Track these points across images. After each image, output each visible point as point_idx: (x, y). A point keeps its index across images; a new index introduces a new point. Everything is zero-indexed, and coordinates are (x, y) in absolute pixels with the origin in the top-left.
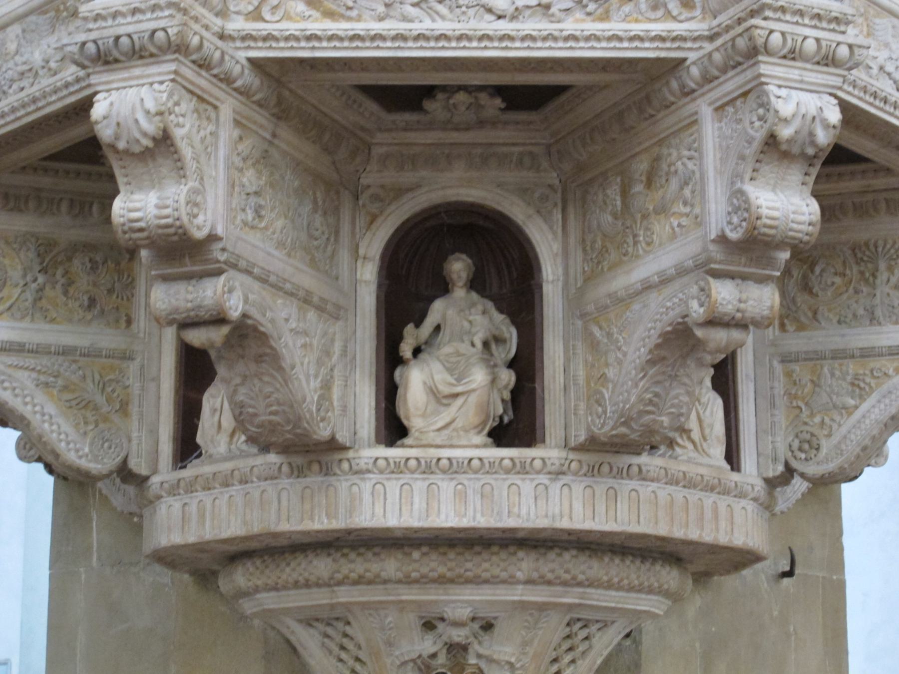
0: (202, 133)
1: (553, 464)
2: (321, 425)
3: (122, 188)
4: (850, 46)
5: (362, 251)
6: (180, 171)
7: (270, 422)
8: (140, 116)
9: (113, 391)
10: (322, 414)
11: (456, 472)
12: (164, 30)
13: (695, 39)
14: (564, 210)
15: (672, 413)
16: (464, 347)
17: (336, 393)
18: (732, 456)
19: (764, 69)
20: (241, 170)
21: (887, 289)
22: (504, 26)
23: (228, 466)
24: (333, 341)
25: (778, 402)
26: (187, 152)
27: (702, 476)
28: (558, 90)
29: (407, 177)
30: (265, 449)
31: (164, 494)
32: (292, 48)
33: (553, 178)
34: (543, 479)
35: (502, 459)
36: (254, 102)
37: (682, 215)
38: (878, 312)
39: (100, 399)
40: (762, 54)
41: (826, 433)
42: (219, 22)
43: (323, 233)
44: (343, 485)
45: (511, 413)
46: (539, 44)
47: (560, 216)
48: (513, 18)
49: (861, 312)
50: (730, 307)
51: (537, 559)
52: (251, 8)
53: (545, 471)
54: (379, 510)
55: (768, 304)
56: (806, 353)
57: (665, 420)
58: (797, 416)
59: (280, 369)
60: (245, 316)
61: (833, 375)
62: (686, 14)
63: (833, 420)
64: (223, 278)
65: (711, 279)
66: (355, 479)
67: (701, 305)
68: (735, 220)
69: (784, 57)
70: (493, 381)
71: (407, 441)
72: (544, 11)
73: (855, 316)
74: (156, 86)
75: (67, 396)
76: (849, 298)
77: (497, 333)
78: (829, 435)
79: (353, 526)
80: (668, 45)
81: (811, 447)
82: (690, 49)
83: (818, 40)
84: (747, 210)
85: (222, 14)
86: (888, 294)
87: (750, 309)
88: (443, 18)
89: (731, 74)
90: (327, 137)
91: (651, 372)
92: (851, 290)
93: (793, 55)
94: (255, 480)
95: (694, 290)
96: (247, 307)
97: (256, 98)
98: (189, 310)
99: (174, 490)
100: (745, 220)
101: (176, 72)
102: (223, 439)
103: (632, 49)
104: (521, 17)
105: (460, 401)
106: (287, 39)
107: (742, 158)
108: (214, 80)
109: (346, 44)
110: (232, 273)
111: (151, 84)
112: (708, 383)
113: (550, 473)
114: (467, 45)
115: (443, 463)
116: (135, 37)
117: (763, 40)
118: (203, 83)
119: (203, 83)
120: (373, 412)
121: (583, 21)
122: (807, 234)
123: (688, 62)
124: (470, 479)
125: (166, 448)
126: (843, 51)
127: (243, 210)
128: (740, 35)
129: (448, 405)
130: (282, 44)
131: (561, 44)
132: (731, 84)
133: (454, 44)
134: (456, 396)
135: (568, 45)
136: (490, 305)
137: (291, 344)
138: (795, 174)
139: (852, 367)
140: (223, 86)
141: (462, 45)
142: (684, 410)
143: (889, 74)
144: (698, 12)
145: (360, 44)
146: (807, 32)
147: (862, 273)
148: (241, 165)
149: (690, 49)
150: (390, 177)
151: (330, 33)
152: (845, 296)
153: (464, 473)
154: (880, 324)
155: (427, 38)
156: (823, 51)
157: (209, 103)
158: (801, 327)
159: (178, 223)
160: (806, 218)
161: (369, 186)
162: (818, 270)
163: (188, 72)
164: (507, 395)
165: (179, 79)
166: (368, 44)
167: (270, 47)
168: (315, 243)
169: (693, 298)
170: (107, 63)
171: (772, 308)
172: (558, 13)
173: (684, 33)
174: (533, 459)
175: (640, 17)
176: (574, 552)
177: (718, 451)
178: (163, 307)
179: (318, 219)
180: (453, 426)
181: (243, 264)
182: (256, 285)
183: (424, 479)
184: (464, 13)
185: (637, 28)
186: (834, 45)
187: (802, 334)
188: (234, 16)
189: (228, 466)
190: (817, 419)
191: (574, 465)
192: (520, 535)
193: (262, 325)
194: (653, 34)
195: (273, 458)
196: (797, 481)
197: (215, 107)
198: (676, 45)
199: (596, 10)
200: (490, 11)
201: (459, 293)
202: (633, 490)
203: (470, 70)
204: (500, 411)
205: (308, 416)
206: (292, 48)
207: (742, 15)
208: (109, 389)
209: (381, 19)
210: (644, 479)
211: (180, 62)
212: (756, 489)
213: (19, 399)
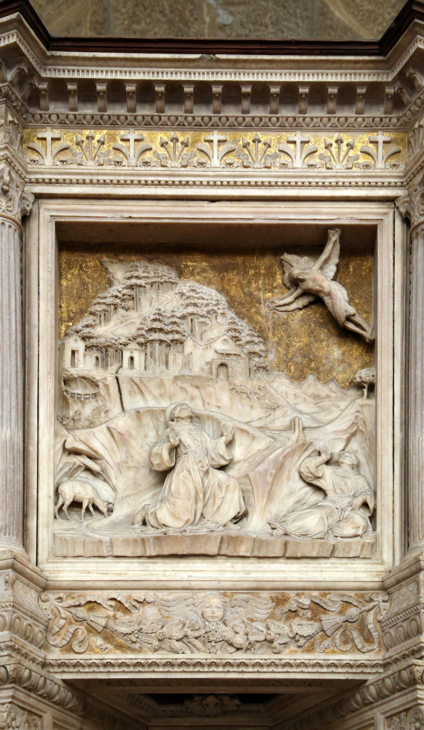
13: (373, 666)
22: (241, 656)
32: (94, 672)
40: (419, 684)
46: (265, 669)
48: (248, 649)
52: (64, 642)
62: (368, 647)
72: (269, 645)
80: (354, 670)
85: (45, 646)
88: (198, 650)
103: (329, 673)
104: (252, 649)
108: (40, 698)
109: (131, 669)
114: (216, 670)
117: (420, 674)
121: (296, 651)
128: (405, 669)
130: (87, 670)
131: (280, 669)
133: (206, 669)
135: (285, 670)
140: (46, 701)
141: (211, 670)
144: (375, 646)
145: (141, 669)
151: (120, 661)
155: (188, 665)
165: (15, 701)
166: (146, 669)
167: (79, 672)
172: (278, 646)
173: (365, 662)
175: (335, 650)
188: (53, 648)
194: (344, 662)
197: (40, 717)
198: (359, 670)
199: (305, 643)
200: (231, 645)
203: (217, 685)
206: (94, 672)
207: (407, 652)
209: (156, 650)
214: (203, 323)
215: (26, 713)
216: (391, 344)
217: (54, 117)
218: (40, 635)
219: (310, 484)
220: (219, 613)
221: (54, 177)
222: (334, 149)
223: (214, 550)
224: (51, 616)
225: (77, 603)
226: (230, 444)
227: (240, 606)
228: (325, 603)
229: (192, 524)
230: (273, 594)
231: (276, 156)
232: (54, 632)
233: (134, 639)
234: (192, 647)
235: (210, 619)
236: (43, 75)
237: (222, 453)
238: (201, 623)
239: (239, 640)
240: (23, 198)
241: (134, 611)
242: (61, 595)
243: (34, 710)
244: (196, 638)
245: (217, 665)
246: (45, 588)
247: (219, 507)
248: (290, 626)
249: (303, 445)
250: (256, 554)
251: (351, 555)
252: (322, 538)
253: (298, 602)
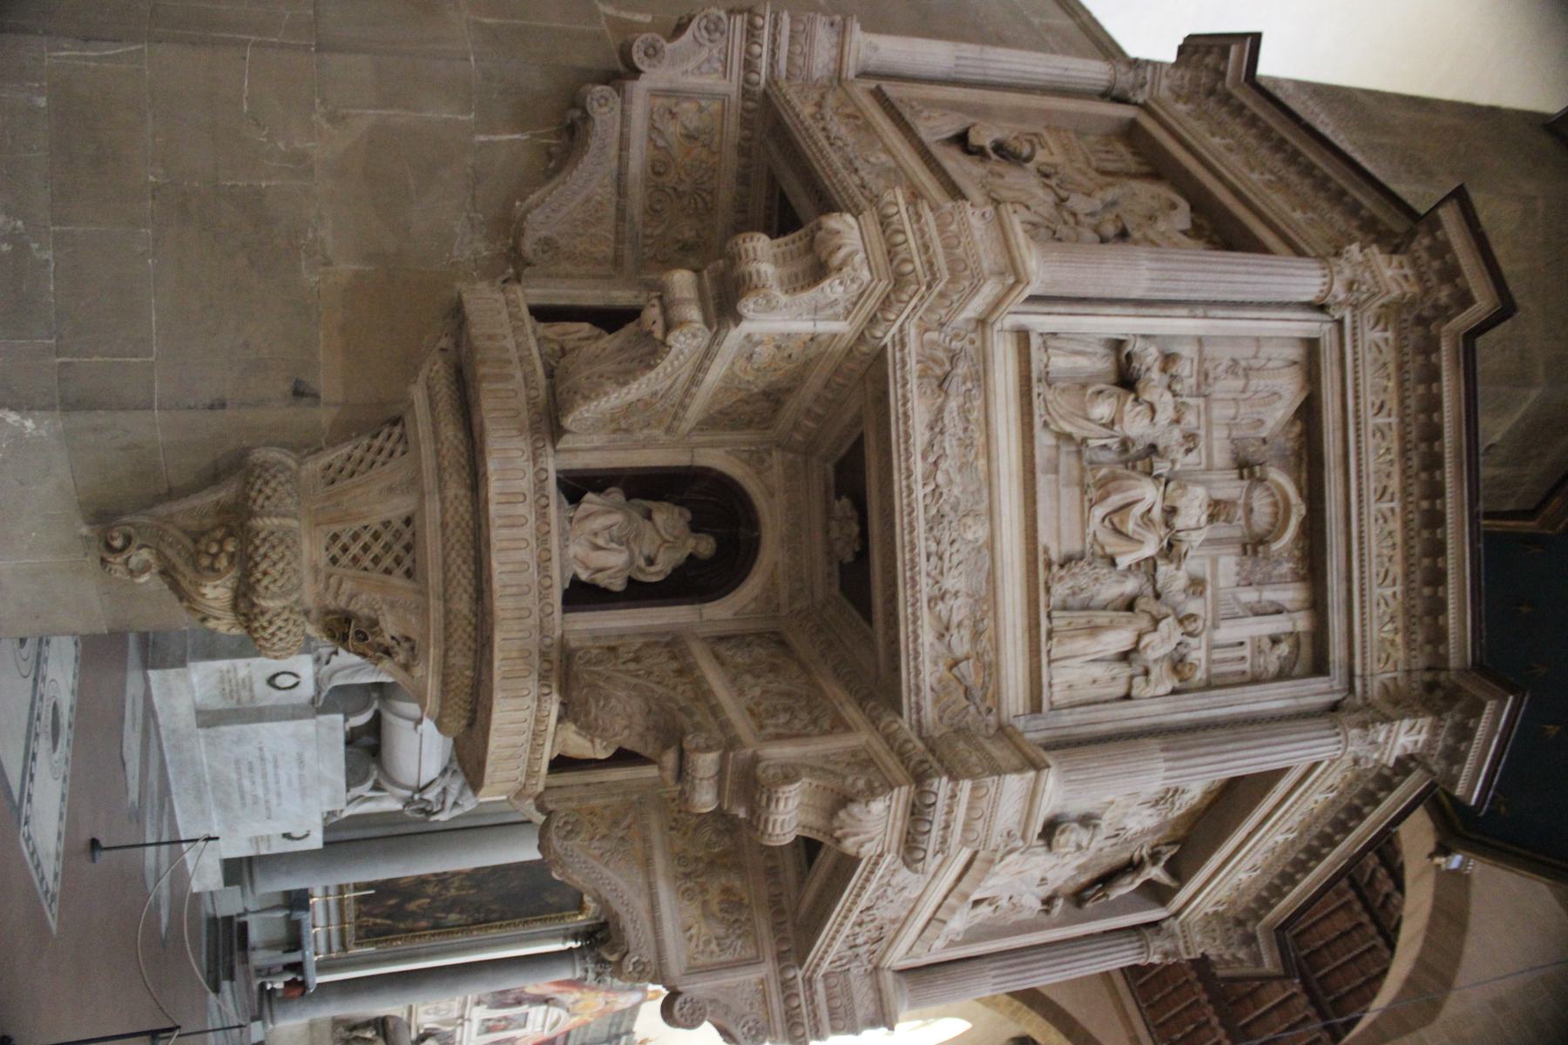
28: (866, 612)
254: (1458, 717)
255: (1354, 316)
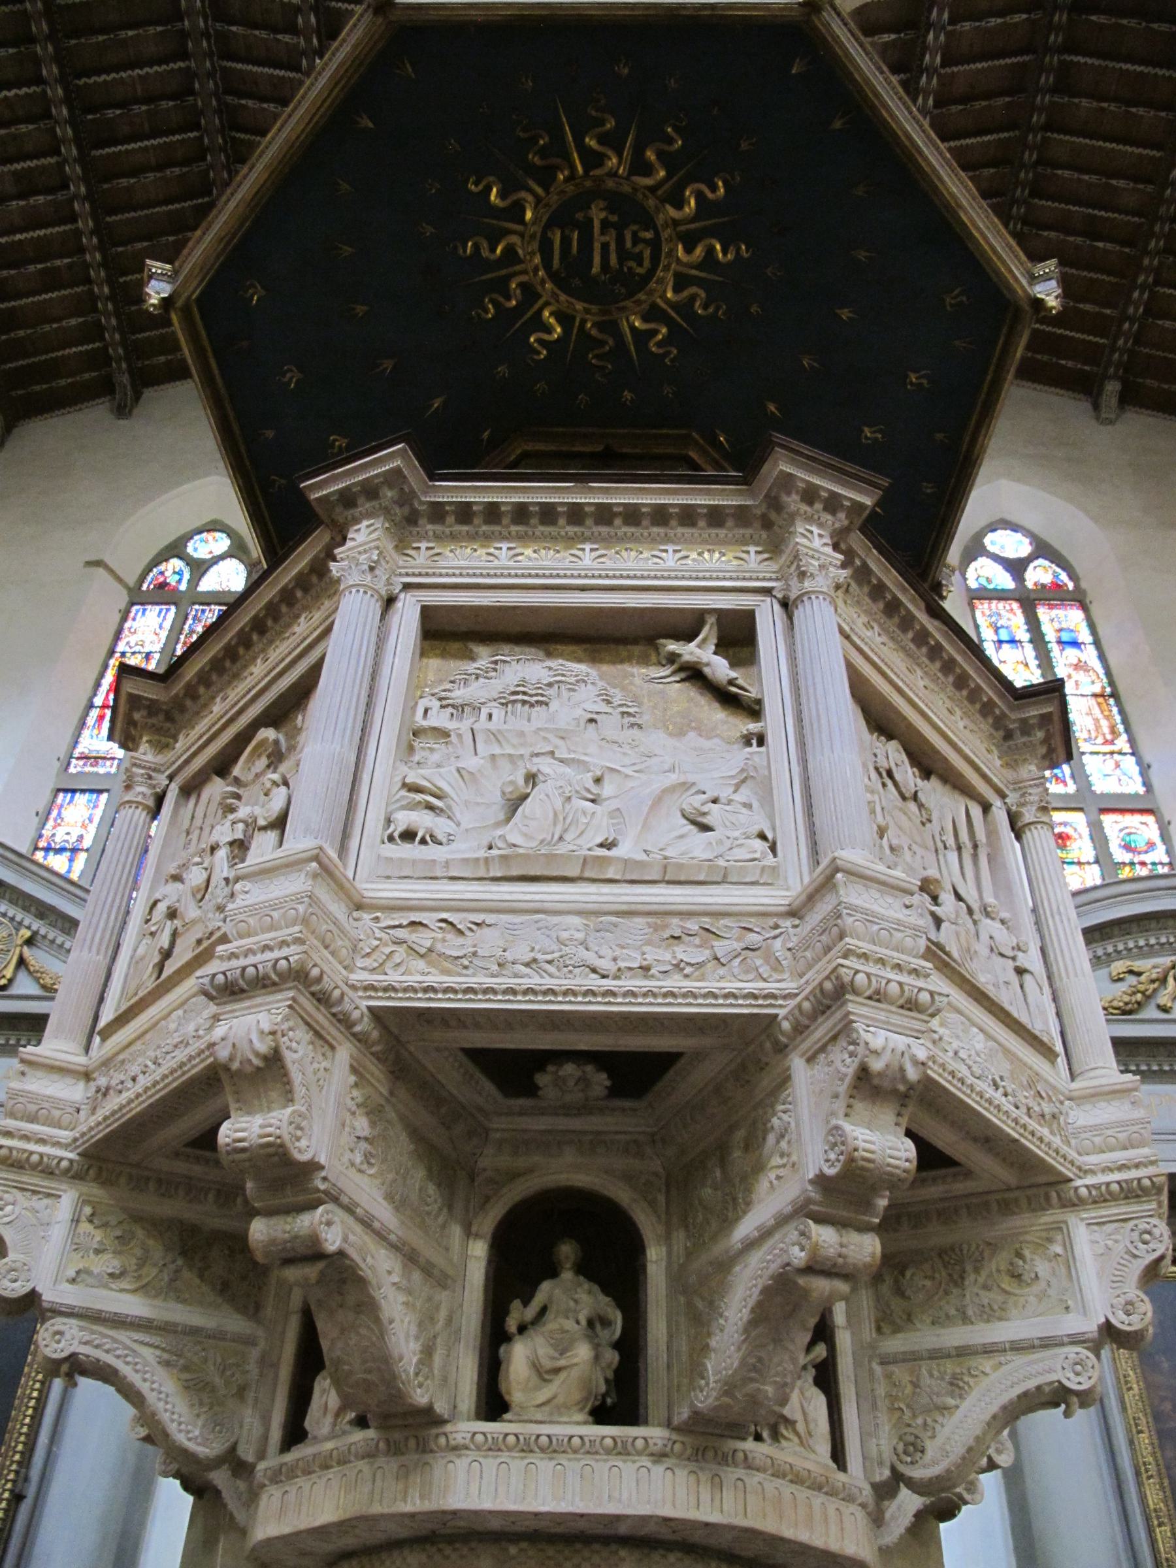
0: (316, 1065)
1: (655, 1444)
2: (419, 1391)
3: (232, 1114)
4: (932, 994)
5: (474, 1229)
6: (288, 1097)
7: (365, 1380)
8: (254, 1037)
9: (233, 1375)
10: (421, 1379)
11: (555, 1451)
12: (286, 958)
14: (668, 1192)
15: (775, 1382)
16: (569, 1324)
17: (437, 1360)
18: (838, 1455)
19: (851, 1007)
20: (354, 1113)
21: (975, 1290)
23: (329, 1445)
24: (437, 1308)
25: (879, 1403)
26: (296, 1077)
27: (809, 1471)
29: (521, 1162)
30: (361, 1422)
31: (267, 1482)
33: (656, 1165)
34: (646, 1461)
35: (603, 1438)
36: (372, 1054)
37: (779, 1167)
38: (970, 1312)
39: (218, 1381)
41: (929, 1434)
42: (344, 972)
43: (436, 1201)
44: (439, 1466)
45: (614, 1395)
47: (663, 1200)
48: (616, 978)
49: (953, 1312)
50: (832, 1250)
51: (641, 1560)
53: (647, 1452)
54: (474, 1489)
55: (870, 1249)
56: (904, 1353)
57: (770, 1390)
58: (900, 1418)
59: (377, 1320)
60: (341, 1253)
61: (931, 1376)
62: (776, 976)
63: (936, 1421)
64: (321, 1209)
65: (810, 1222)
66: (451, 1456)
67: (802, 1249)
68: (832, 1156)
69: (870, 998)
70: (597, 1358)
71: (506, 1416)
73: (947, 1316)
74: (274, 1011)
75: (186, 1376)
76: (940, 1300)
77: (602, 1313)
78: (933, 1437)
79: (446, 1508)
80: (760, 1002)
81: (916, 1450)
82: (781, 1006)
83: (900, 984)
84: (843, 1143)
86: (977, 1294)
87: (851, 1253)
88: (551, 976)
89: (820, 1020)
90: (443, 1110)
91: (753, 1334)
92: (941, 1292)
93: (878, 997)
94: (352, 1459)
95: (794, 1235)
96: (346, 1246)
97: (376, 1049)
98: (285, 1242)
99: (278, 1476)
100: (842, 1154)
101: (294, 999)
102: (329, 1419)
105: (563, 1375)
106: (405, 990)
107: (836, 1096)
109: (460, 996)
110: (330, 1206)
111: (269, 1010)
112: (811, 1380)
113: (652, 1455)
115: (544, 1440)
116: (260, 967)
118: (320, 1018)
119: (320, 1018)
120: (475, 1386)
122: (904, 1171)
123: (780, 1017)
124: (569, 1460)
125: (276, 1435)
126: (924, 997)
127: (352, 1151)
129: (550, 1381)
132: (821, 1030)
134: (557, 1371)
136: (596, 1288)
137: (391, 1297)
138: (887, 1115)
139: (950, 1367)
142: (788, 1380)
143: (963, 1060)
146: (891, 976)
147: (950, 1275)
148: (354, 1108)
149: (781, 1006)
150: (505, 1161)
152: (936, 1298)
153: (564, 1452)
154: (972, 1323)
156: (907, 994)
157: (327, 1042)
158: (897, 1330)
159: (279, 1141)
160: (903, 1155)
161: (485, 1170)
162: (908, 1274)
163: (307, 1003)
164: (610, 1375)
168: (427, 1208)
169: (793, 1245)
170: (233, 993)
171: (873, 1255)
174: (636, 1438)
176: (679, 1555)
177: (824, 1448)
178: (262, 1238)
179: (431, 1189)
180: (556, 1401)
181: (344, 1200)
182: (358, 1228)
183: (522, 1458)
184: (570, 972)
185: (731, 986)
186: (916, 990)
187: (900, 1335)
189: (329, 1445)
190: (920, 1421)
191: (677, 1447)
192: (623, 1529)
193: (361, 1269)
195: (371, 1433)
196: (904, 1492)
197: (333, 1048)
198: (768, 1002)
200: (594, 971)
201: (567, 1275)
202: (739, 1479)
204: (603, 1388)
205: (404, 1377)
208: (228, 1373)
209: (493, 976)
210: (749, 1467)
211: (299, 990)
212: (864, 1493)
213: (147, 1384)
214: (570, 690)
215: (311, 1033)
216: (779, 695)
217: (431, 533)
218: (344, 951)
219: (694, 822)
220: (580, 936)
221: (423, 571)
222: (706, 555)
223: (574, 872)
224: (362, 937)
225: (397, 923)
226: (598, 781)
227: (607, 931)
228: (718, 928)
229: (549, 844)
230: (649, 920)
231: (648, 559)
232: (363, 953)
233: (466, 963)
234: (541, 972)
235: (567, 942)
236: (423, 499)
237: (587, 786)
238: (555, 947)
239: (605, 964)
240: (389, 583)
241: (468, 933)
242: (379, 914)
243: (323, 1032)
244: (549, 962)
245: (575, 994)
246: (359, 907)
247: (582, 833)
248: (674, 952)
249: (684, 783)
250: (628, 877)
251: (747, 880)
252: (710, 860)
253: (682, 927)
254: (795, 497)
255: (400, 575)
